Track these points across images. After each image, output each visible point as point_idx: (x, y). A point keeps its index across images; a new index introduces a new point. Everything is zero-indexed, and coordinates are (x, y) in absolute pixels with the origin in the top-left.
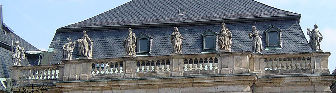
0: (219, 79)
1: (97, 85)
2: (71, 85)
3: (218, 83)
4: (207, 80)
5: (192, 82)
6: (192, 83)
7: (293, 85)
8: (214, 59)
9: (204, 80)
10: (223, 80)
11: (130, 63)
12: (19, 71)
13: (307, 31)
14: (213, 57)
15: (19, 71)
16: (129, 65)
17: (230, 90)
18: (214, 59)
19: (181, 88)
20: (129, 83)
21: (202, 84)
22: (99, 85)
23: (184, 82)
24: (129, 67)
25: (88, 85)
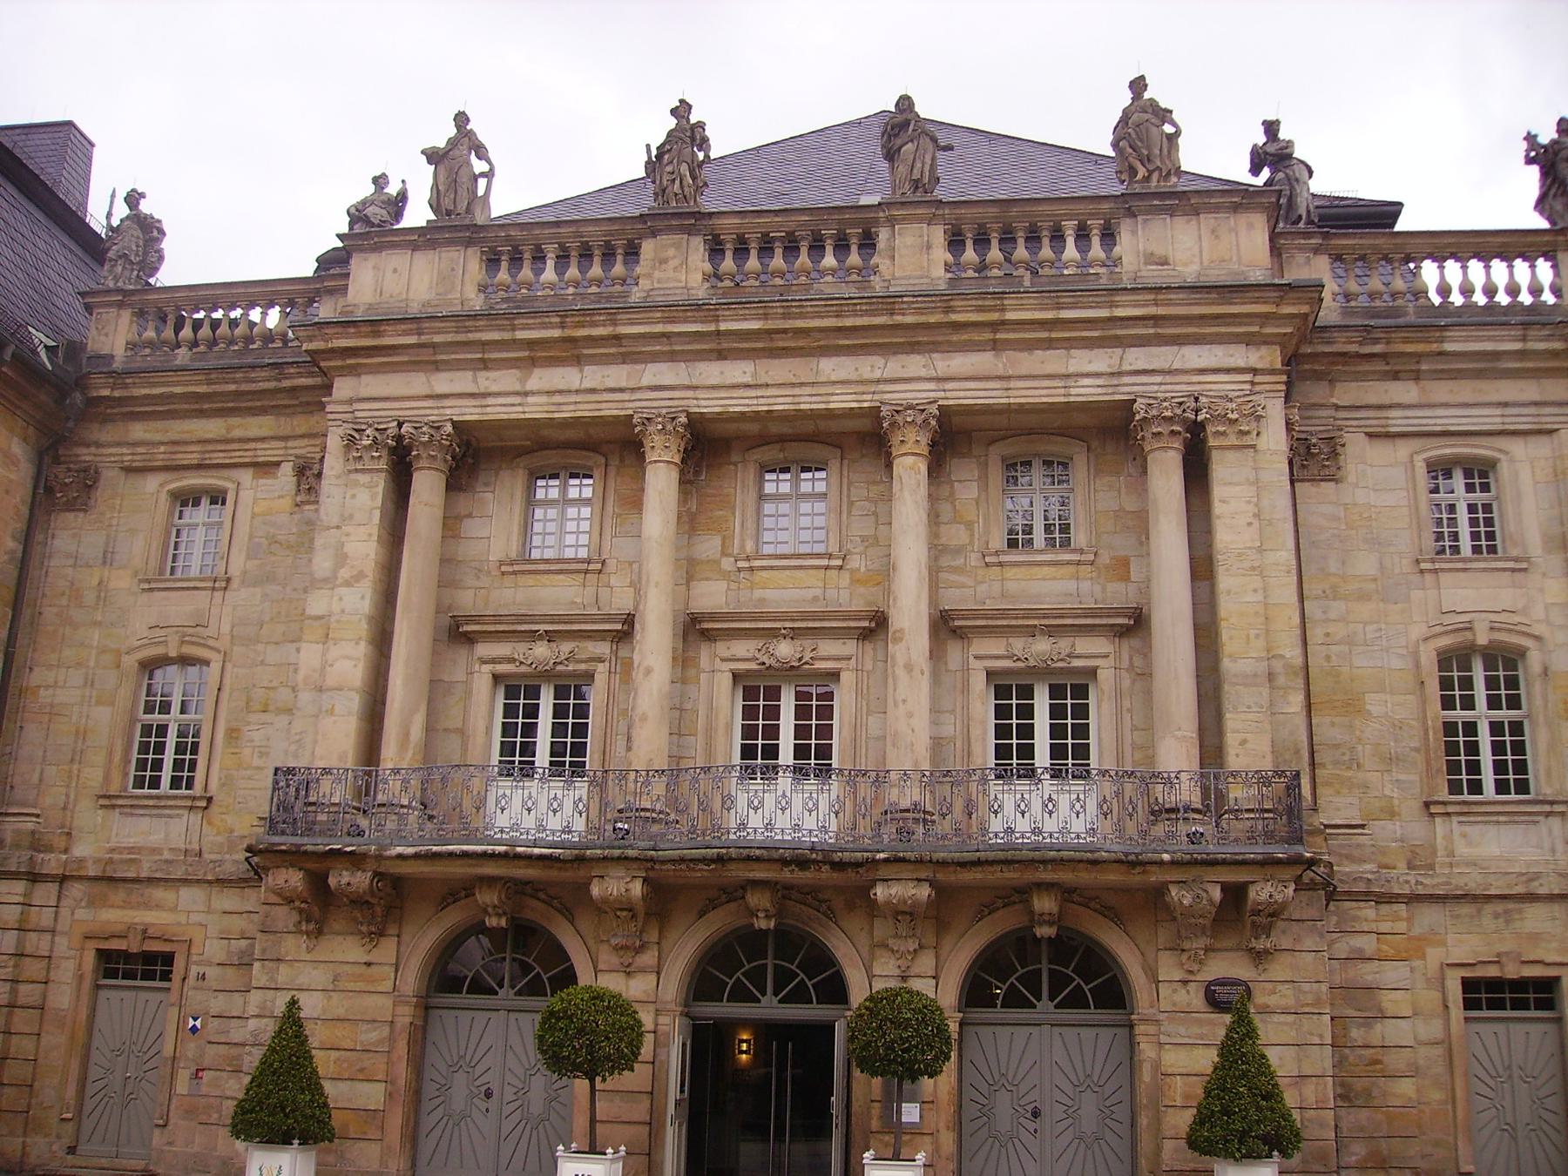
0: (1136, 305)
1: (506, 336)
2: (377, 334)
3: (1127, 327)
4: (1073, 306)
5: (995, 316)
6: (995, 326)
7: (1479, 374)
8: (1095, 224)
9: (1059, 307)
10: (1152, 310)
11: (677, 246)
12: (126, 315)
13: (1525, 145)
14: (1093, 215)
15: (126, 315)
16: (671, 252)
17: (1188, 366)
18: (1095, 224)
19: (934, 355)
20: (672, 321)
21: (1045, 335)
22: (520, 335)
23: (954, 317)
24: (673, 263)
25: (461, 337)
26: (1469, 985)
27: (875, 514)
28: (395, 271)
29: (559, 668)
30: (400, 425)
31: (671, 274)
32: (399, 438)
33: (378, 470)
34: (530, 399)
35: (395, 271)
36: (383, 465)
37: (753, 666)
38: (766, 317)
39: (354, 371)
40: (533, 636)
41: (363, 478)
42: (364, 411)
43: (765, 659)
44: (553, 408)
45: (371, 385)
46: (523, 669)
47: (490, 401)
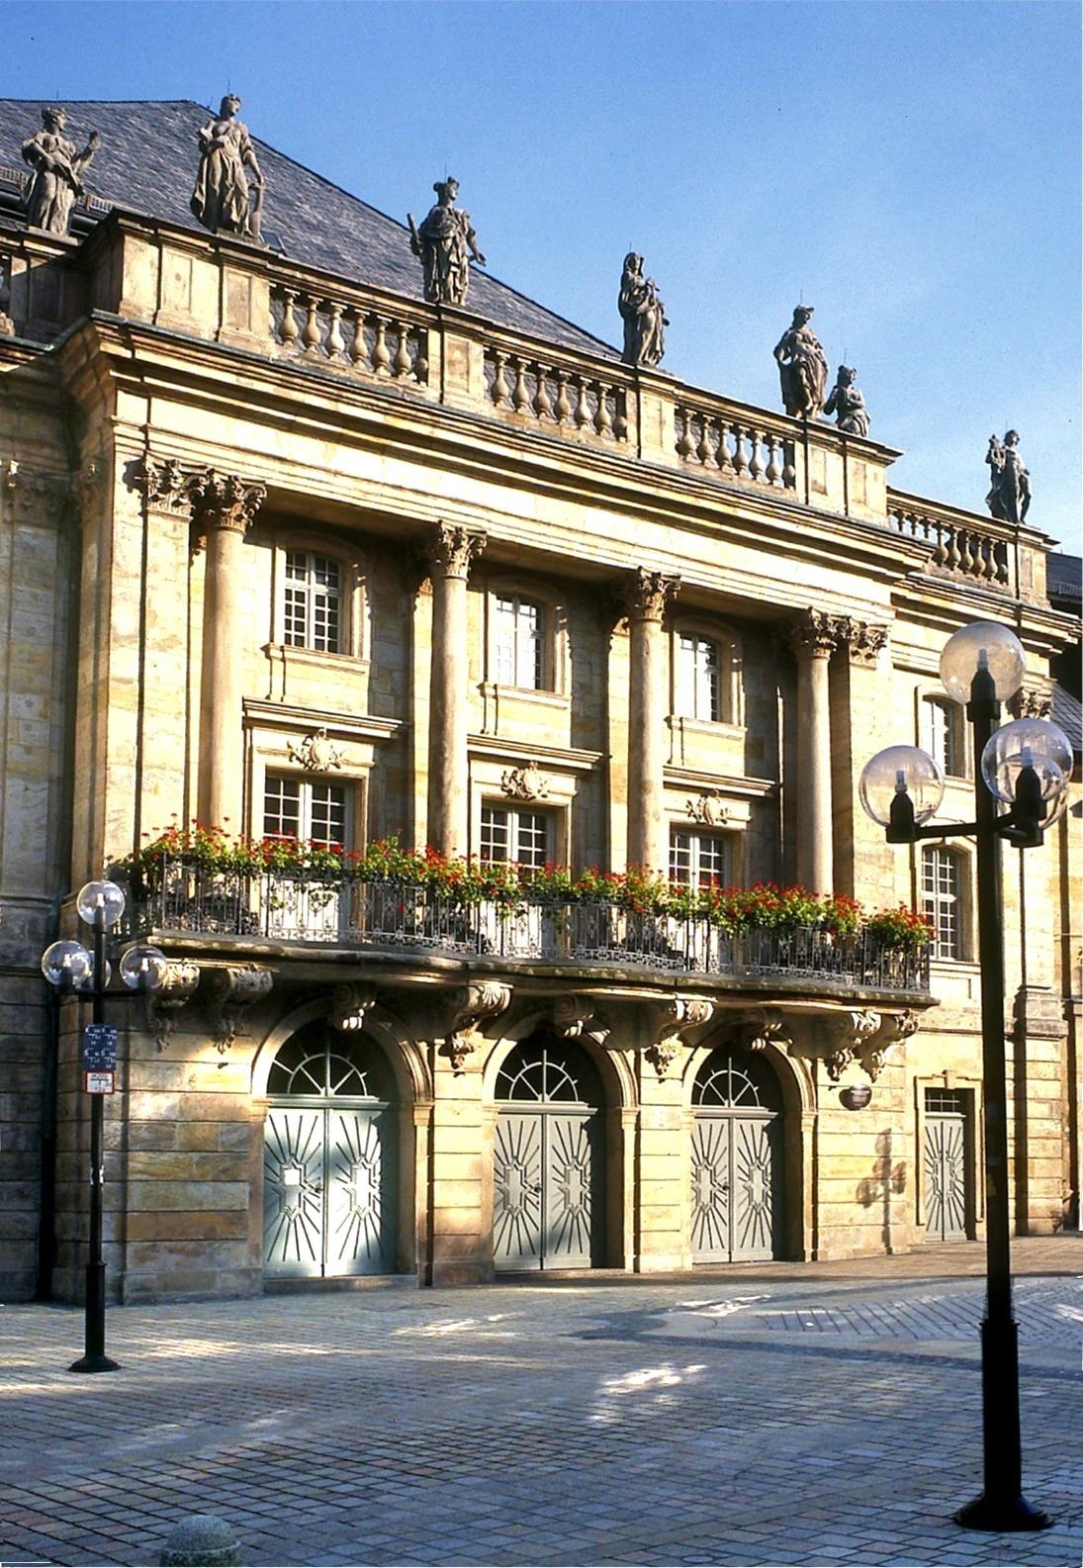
16: (457, 355)
26: (929, 1092)
27: (589, 663)
28: (178, 277)
29: (333, 769)
30: (211, 472)
31: (457, 379)
32: (211, 488)
33: (184, 520)
34: (340, 480)
35: (178, 277)
36: (185, 512)
37: (497, 792)
38: (564, 460)
39: (147, 392)
40: (311, 732)
41: (167, 525)
42: (163, 447)
43: (513, 786)
44: (360, 495)
45: (167, 413)
46: (296, 765)
47: (297, 470)
